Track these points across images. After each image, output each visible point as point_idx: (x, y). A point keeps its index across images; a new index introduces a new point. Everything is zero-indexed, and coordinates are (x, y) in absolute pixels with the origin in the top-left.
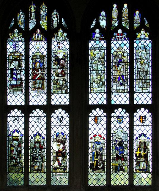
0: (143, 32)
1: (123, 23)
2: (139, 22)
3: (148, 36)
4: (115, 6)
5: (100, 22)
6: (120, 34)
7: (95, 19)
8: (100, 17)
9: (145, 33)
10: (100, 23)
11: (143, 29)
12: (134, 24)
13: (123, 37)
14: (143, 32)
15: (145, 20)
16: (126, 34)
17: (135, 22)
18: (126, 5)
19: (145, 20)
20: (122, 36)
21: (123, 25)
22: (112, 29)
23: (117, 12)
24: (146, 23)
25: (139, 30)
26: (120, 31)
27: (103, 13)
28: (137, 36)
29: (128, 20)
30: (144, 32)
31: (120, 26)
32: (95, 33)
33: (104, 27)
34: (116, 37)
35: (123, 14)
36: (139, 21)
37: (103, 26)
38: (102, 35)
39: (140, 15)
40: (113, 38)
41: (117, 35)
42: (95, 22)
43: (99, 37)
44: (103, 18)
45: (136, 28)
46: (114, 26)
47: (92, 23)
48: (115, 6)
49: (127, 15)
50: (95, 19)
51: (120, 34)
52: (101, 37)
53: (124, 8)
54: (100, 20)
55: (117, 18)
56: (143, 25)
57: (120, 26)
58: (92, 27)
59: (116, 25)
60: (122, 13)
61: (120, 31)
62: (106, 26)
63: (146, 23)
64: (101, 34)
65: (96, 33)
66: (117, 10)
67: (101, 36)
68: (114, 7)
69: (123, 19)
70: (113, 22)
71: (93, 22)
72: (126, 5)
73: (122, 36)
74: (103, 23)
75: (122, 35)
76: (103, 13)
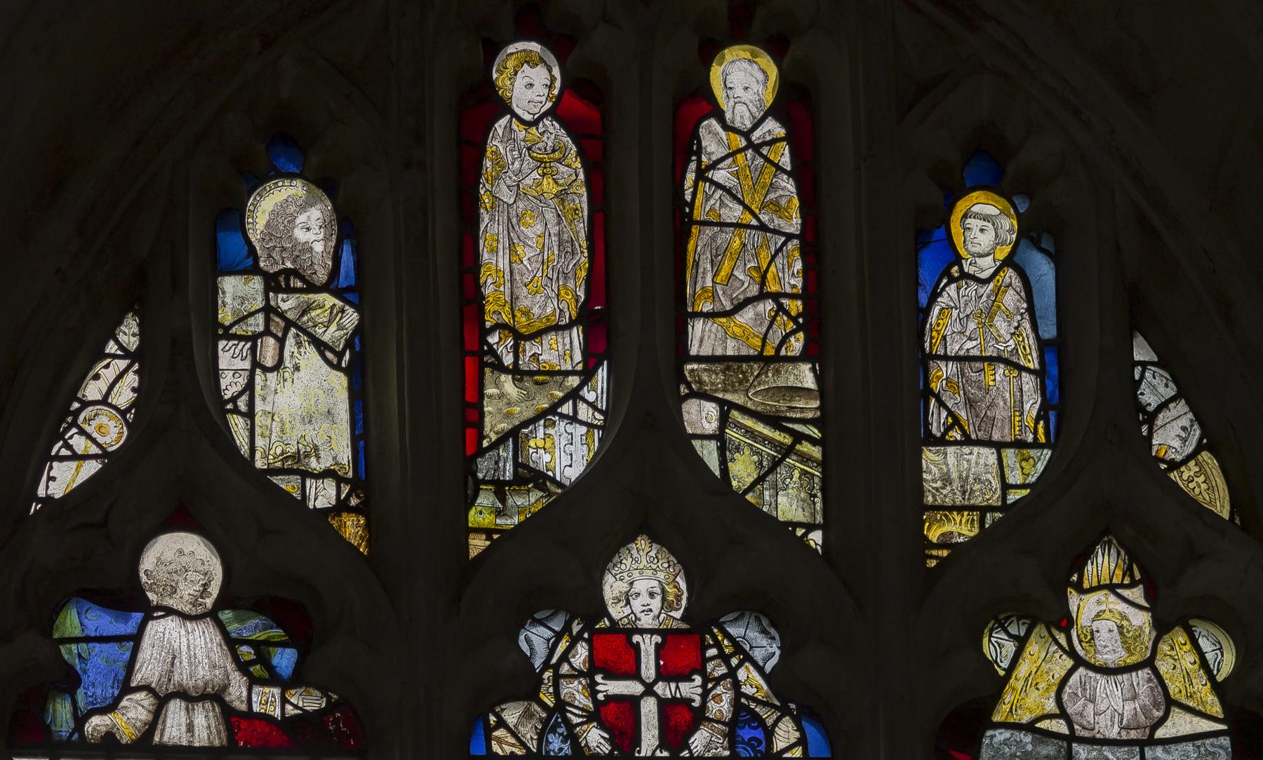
0: (1107, 612)
1: (700, 417)
2: (1032, 405)
3: (1216, 709)
4: (529, 81)
5: (230, 384)
6: (648, 646)
7: (129, 334)
8: (238, 294)
9: (1162, 627)
10: (222, 407)
11: (1104, 564)
12: (930, 456)
13: (721, 706)
14: (1107, 612)
15: (1155, 388)
16: (767, 649)
17: (937, 421)
18: (744, 81)
19: (1155, 388)
20: (690, 689)
21: (709, 453)
22: (478, 544)
23: (581, 198)
24: (1173, 434)
25: (1026, 568)
26: (641, 586)
27: (291, 217)
28: (996, 685)
29: (806, 376)
30: (1141, 620)
31: (648, 481)
32: (131, 600)
33: (323, 495)
34: (575, 691)
35: (699, 242)
36: (1017, 399)
37: (296, 466)
38: (285, 660)
39: (1043, 270)
40: (512, 714)
41: (598, 665)
42: (124, 396)
43: (215, 696)
44: (287, 303)
45: (962, 528)
46: (529, 477)
47: (57, 412)
48: (529, 81)
49: (790, 275)
50: (129, 334)
51: (648, 646)
52: (267, 701)
53: (712, 139)
54: (231, 361)
55: (587, 318)
56: (1092, 491)
57: (648, 481)
58: (62, 479)
59: (566, 453)
60: (681, 222)
61: (641, 586)
62: (364, 481)
63: (1173, 434)
64: (252, 627)
65: (150, 612)
66: (572, 169)
67: (258, 671)
68: (503, 107)
69: (703, 337)
70: (503, 401)
71: (93, 391)
72: (744, 81)
73: (690, 689)
74: (297, 409)
75: (683, 649)
76: (291, 217)
